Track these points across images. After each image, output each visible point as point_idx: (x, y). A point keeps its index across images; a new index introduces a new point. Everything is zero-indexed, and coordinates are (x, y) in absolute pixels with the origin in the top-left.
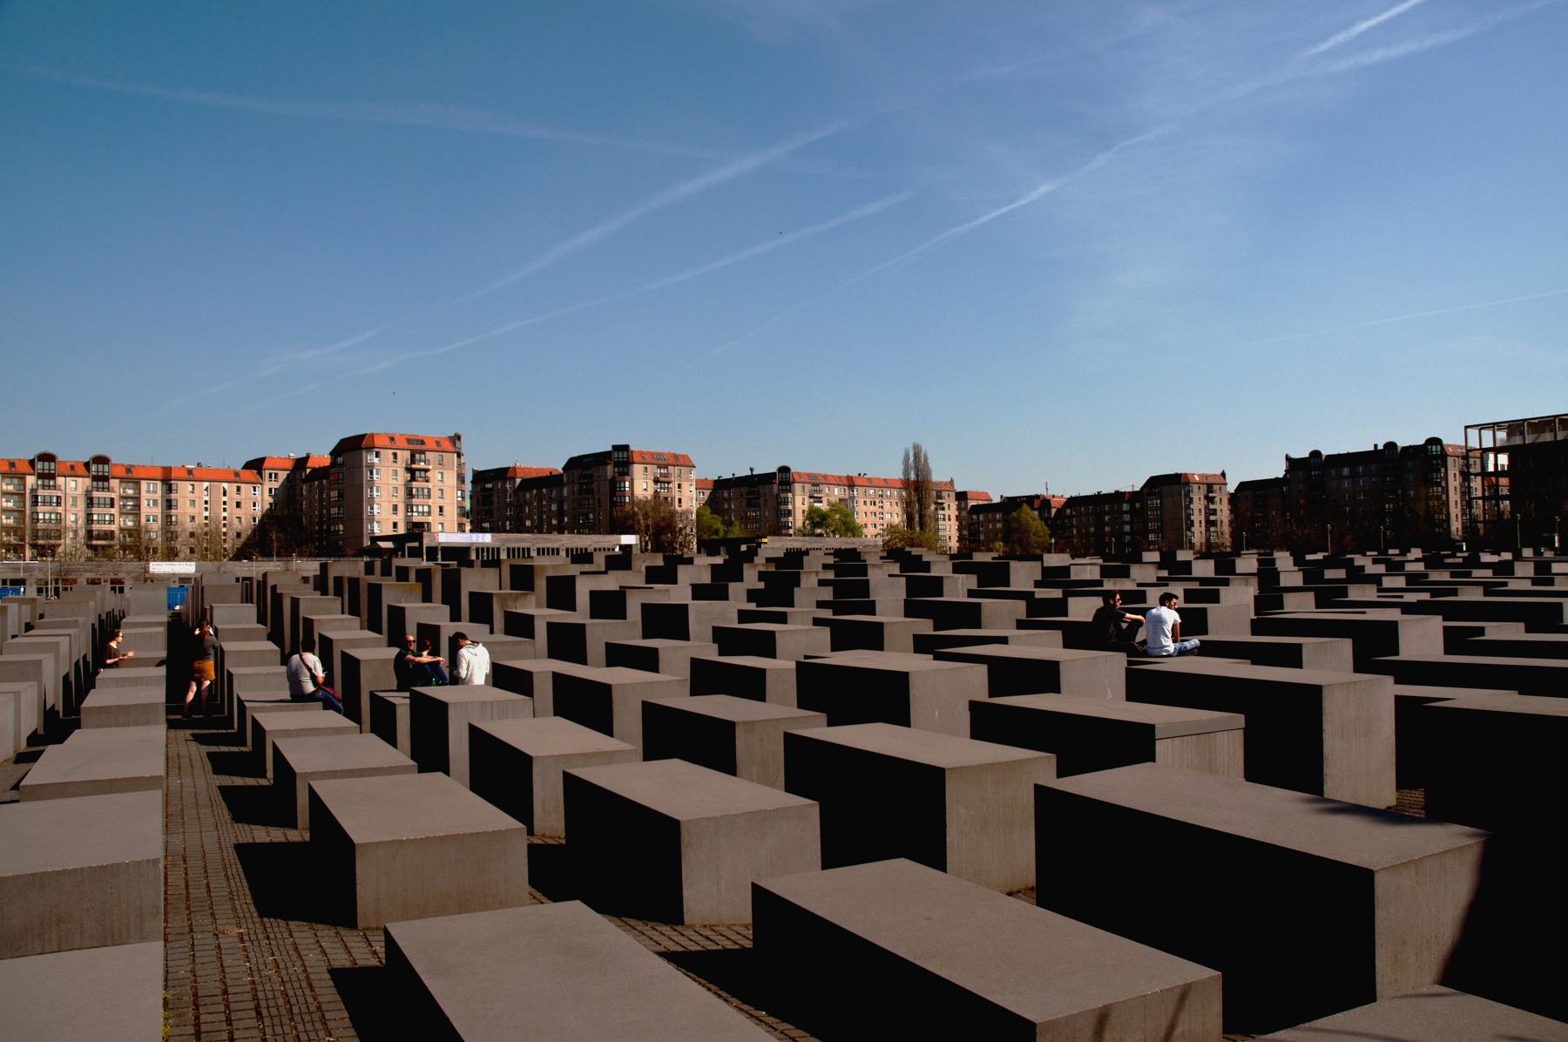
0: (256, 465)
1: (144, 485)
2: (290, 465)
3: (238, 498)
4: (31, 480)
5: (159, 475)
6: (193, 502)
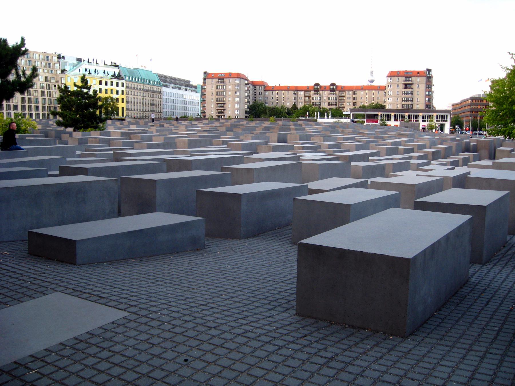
4: (312, 92)
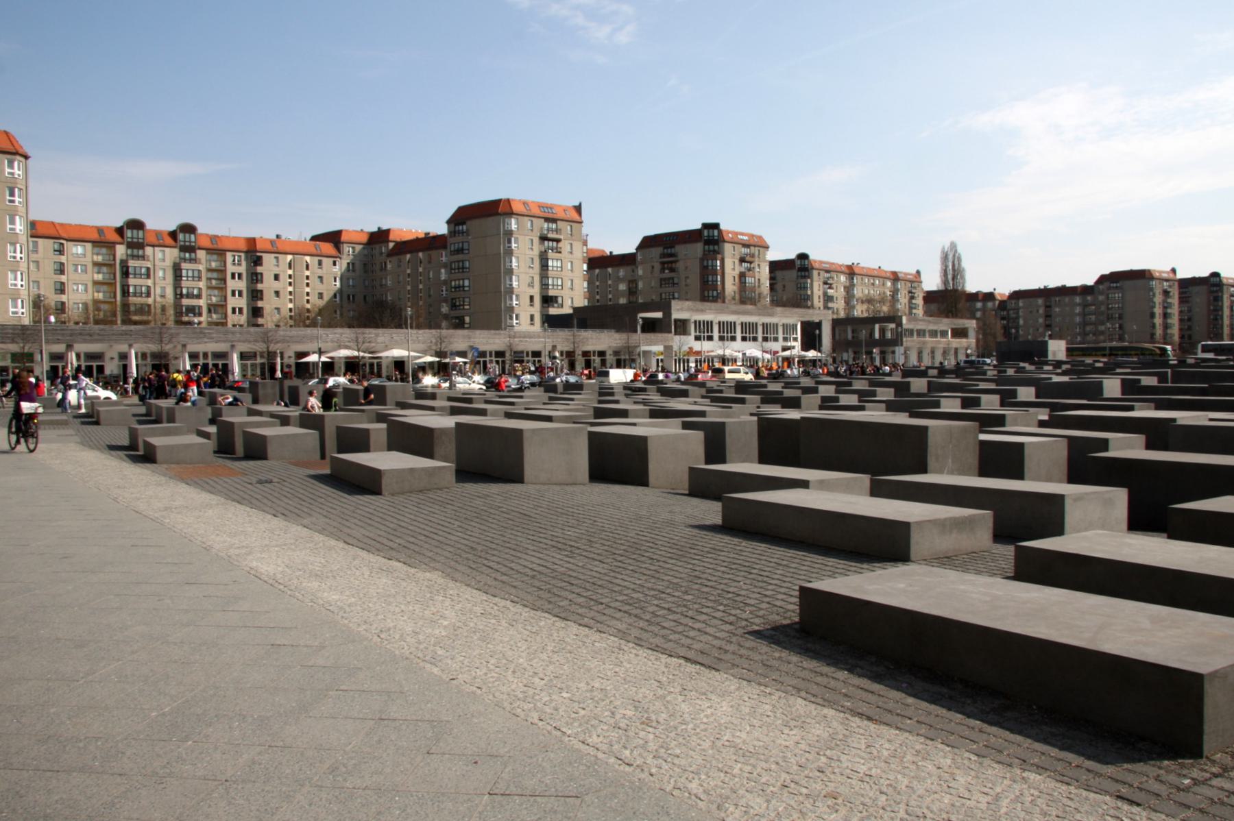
0: (334, 238)
1: (229, 256)
2: (365, 239)
3: (320, 272)
4: (121, 250)
5: (243, 247)
6: (277, 277)
